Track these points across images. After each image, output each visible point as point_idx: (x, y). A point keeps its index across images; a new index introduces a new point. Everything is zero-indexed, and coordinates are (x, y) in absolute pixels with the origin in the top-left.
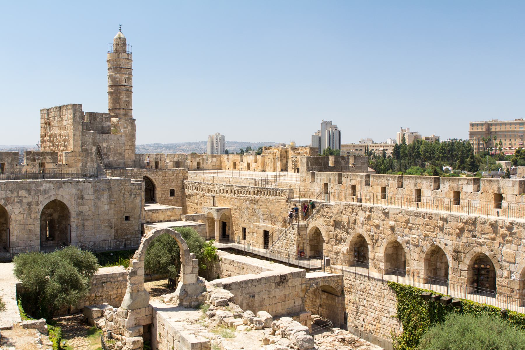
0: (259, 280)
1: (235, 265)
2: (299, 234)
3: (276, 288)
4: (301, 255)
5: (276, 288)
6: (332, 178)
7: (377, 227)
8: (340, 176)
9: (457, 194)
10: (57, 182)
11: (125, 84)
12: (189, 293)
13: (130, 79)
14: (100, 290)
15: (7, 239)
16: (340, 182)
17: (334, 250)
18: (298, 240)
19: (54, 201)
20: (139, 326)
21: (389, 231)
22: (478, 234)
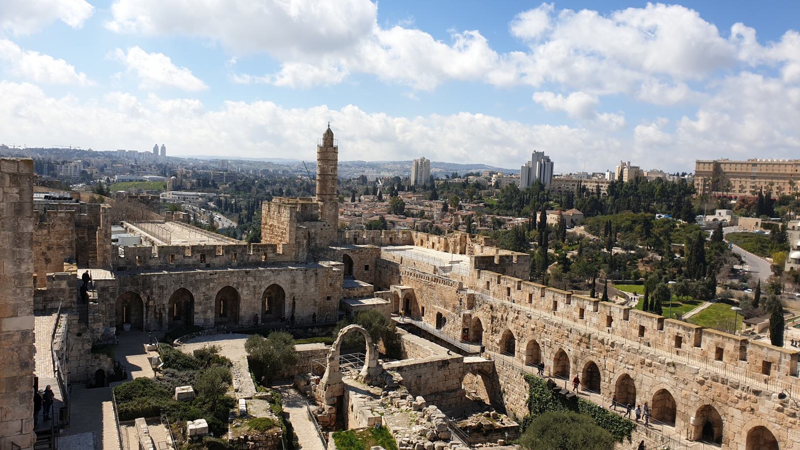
0: (425, 364)
1: (411, 345)
2: (464, 321)
3: (438, 370)
4: (465, 339)
5: (438, 370)
6: (493, 278)
7: (523, 326)
8: (499, 277)
9: (582, 311)
10: (276, 270)
11: (331, 173)
12: (371, 374)
13: (335, 169)
14: (306, 361)
15: (236, 313)
16: (499, 282)
17: (490, 339)
18: (463, 326)
19: (274, 285)
20: (334, 397)
21: (530, 332)
22: (591, 347)
